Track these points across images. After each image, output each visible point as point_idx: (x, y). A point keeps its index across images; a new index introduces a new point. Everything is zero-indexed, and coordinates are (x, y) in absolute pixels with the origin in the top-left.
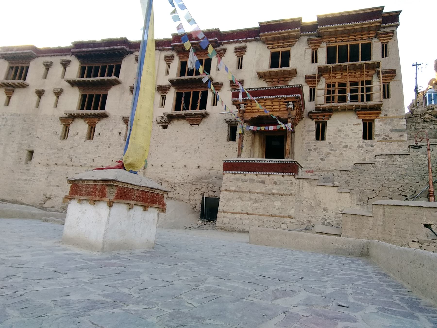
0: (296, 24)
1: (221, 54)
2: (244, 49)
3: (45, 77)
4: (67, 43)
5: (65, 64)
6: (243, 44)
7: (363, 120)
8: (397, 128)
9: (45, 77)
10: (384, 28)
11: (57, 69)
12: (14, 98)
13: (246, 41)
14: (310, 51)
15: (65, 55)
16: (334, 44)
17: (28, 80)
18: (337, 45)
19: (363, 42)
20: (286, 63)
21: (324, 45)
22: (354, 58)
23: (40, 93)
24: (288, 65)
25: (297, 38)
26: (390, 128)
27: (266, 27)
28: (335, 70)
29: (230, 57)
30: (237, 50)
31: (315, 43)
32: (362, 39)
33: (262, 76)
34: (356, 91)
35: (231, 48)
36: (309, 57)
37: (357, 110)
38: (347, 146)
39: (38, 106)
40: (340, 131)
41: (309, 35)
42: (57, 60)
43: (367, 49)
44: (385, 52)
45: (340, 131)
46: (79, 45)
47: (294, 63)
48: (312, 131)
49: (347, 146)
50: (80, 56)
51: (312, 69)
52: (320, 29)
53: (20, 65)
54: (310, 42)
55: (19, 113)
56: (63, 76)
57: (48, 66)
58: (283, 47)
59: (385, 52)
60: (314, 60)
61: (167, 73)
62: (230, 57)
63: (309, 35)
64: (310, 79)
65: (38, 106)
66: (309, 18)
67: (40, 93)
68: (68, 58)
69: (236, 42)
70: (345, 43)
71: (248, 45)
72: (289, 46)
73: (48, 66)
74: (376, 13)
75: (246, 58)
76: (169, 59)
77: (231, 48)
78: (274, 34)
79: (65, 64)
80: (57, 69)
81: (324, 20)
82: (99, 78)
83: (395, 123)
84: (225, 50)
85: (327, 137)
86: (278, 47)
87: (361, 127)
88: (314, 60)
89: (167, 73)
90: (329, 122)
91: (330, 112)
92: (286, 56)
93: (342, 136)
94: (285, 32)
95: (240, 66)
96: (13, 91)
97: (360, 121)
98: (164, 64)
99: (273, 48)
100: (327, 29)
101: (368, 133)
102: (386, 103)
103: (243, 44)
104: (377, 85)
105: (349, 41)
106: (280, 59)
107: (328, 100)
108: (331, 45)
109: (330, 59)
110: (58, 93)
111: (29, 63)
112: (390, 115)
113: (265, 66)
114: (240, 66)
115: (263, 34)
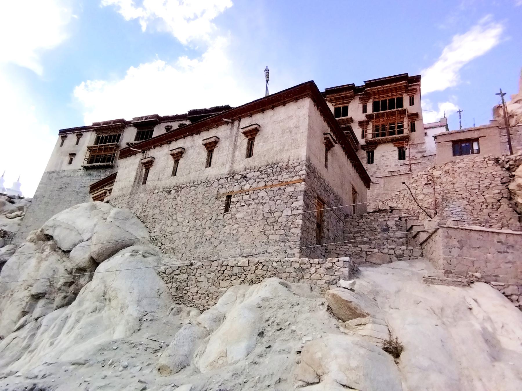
0: (351, 87)
4: (184, 111)
7: (398, 148)
8: (420, 150)
10: (411, 86)
14: (361, 106)
15: (182, 121)
16: (378, 100)
19: (397, 97)
21: (371, 100)
22: (392, 107)
24: (347, 115)
25: (352, 97)
26: (416, 151)
28: (378, 116)
31: (365, 100)
32: (396, 95)
34: (391, 128)
36: (361, 109)
37: (392, 141)
38: (388, 166)
40: (383, 156)
41: (360, 95)
44: (412, 103)
45: (383, 156)
47: (351, 114)
48: (364, 158)
49: (388, 166)
51: (362, 117)
52: (366, 91)
54: (361, 99)
58: (343, 103)
59: (412, 103)
60: (365, 110)
63: (360, 95)
64: (361, 124)
66: (359, 83)
70: (385, 99)
74: (404, 77)
78: (336, 95)
81: (369, 84)
83: (419, 147)
85: (374, 161)
86: (340, 104)
87: (397, 152)
90: (375, 151)
93: (385, 159)
94: (343, 94)
97: (396, 148)
99: (336, 105)
100: (372, 89)
101: (402, 156)
102: (413, 135)
104: (406, 122)
105: (388, 96)
107: (373, 136)
108: (376, 100)
109: (375, 109)
111: (153, 128)
112: (415, 143)
115: (328, 96)
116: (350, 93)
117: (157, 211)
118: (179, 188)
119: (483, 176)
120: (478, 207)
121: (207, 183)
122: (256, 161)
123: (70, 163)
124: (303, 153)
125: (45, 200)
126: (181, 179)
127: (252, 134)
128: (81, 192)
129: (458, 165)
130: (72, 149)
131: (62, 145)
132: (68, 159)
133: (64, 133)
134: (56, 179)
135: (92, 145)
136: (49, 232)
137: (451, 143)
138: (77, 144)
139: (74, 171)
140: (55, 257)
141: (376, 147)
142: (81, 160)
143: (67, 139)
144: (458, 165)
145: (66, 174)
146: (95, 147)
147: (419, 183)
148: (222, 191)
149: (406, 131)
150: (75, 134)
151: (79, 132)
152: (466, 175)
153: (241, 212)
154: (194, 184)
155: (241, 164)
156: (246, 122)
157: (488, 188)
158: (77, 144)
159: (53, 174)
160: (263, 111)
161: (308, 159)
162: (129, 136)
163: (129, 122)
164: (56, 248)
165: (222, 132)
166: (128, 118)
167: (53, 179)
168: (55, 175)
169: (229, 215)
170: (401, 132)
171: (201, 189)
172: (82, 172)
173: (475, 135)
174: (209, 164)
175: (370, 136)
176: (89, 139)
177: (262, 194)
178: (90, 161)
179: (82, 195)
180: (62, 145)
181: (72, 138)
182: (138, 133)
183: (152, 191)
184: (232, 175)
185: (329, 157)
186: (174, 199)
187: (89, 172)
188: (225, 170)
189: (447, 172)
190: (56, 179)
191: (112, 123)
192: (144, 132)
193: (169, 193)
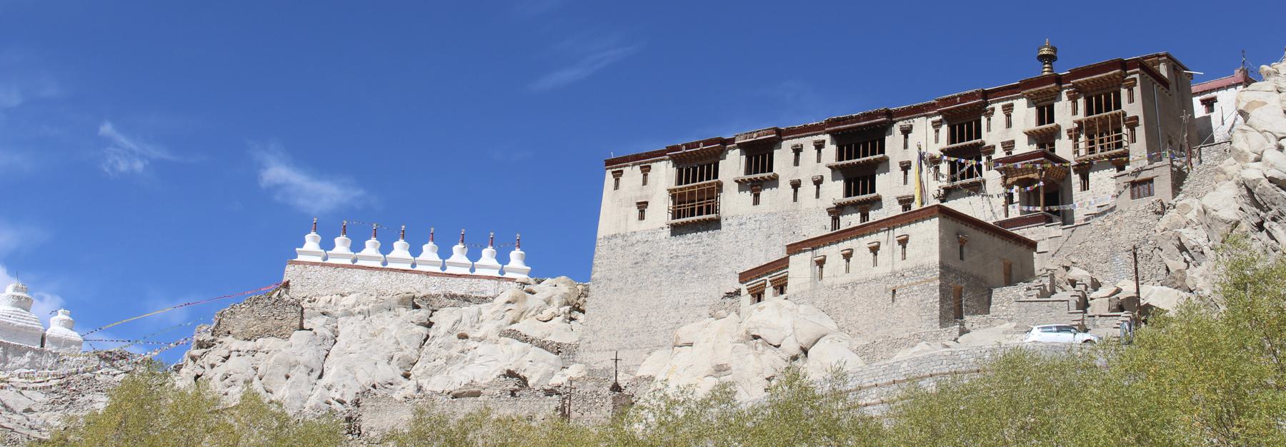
1: (989, 115)
3: (796, 163)
5: (819, 146)
9: (796, 163)
11: (809, 152)
17: (776, 169)
20: (1051, 120)
23: (796, 185)
29: (999, 116)
33: (1032, 136)
35: (998, 107)
39: (795, 199)
55: (773, 210)
56: (819, 161)
57: (797, 151)
60: (1075, 112)
61: (937, 140)
62: (999, 116)
65: (795, 199)
67: (796, 185)
68: (821, 137)
71: (1015, 102)
73: (797, 151)
76: (936, 125)
77: (998, 107)
79: (819, 146)
80: (809, 152)
82: (861, 159)
84: (993, 109)
88: (1075, 112)
89: (937, 140)
95: (1009, 124)
98: (931, 131)
110: (818, 183)
113: (1032, 125)
114: (1009, 124)
117: (839, 304)
118: (854, 284)
121: (876, 279)
122: (909, 264)
123: (642, 217)
124: (936, 259)
125: (615, 285)
126: (855, 275)
127: (903, 242)
128: (674, 267)
130: (638, 194)
134: (623, 248)
135: (673, 186)
138: (645, 183)
139: (654, 233)
140: (770, 352)
142: (661, 211)
145: (638, 237)
148: (889, 286)
149: (1125, 144)
150: (637, 168)
153: (903, 300)
154: (867, 281)
155: (900, 265)
156: (899, 232)
158: (645, 183)
159: (614, 240)
160: (910, 223)
161: (941, 263)
165: (881, 237)
167: (618, 249)
168: (619, 241)
170: (1119, 145)
171: (872, 285)
172: (667, 232)
174: (875, 263)
175: (1082, 152)
177: (915, 288)
178: (677, 214)
179: (676, 270)
183: (831, 287)
184: (894, 273)
185: (965, 250)
186: (852, 293)
188: (889, 270)
189: (1116, 223)
190: (623, 248)
193: (846, 288)
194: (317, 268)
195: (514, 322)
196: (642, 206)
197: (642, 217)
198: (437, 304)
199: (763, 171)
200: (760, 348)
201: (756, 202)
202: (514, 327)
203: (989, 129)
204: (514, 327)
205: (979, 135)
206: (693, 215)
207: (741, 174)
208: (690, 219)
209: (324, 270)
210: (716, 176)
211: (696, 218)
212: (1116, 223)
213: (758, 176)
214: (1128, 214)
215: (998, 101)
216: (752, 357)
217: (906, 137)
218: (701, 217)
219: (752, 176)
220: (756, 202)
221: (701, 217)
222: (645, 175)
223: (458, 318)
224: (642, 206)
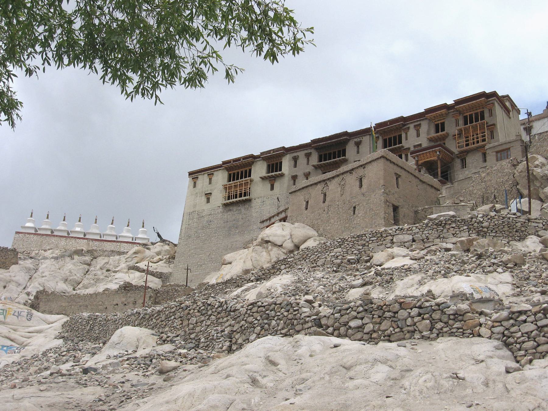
0: (445, 106)
2: (420, 125)
5: (308, 156)
6: (418, 123)
11: (302, 160)
12: (276, 185)
13: (420, 120)
18: (468, 114)
25: (447, 114)
27: (429, 111)
30: (415, 126)
35: (412, 126)
42: (301, 154)
43: (482, 114)
46: (314, 141)
50: (317, 149)
53: (275, 162)
56: (308, 164)
57: (295, 159)
60: (457, 124)
62: (412, 132)
66: (450, 102)
69: (414, 122)
71: (421, 122)
72: (444, 119)
73: (295, 159)
75: (421, 131)
77: (412, 126)
79: (308, 156)
80: (302, 160)
81: (458, 102)
84: (409, 128)
86: (438, 121)
90: (467, 159)
91: (467, 152)
92: (443, 124)
95: (418, 135)
96: (275, 180)
103: (418, 123)
106: (440, 127)
116: (444, 111)
119: (505, 174)
120: (501, 193)
123: (208, 200)
129: (494, 169)
131: (195, 186)
132: (204, 199)
133: (194, 175)
136: (267, 239)
137: (495, 153)
140: (275, 249)
141: (467, 154)
142: (219, 198)
143: (199, 179)
144: (494, 169)
146: (229, 184)
147: (474, 183)
150: (206, 175)
151: (210, 171)
152: (497, 175)
157: (507, 181)
162: (259, 170)
163: (258, 157)
164: (275, 245)
166: (257, 153)
169: (355, 216)
172: (221, 210)
173: (504, 147)
176: (221, 178)
180: (195, 186)
181: (203, 180)
182: (269, 166)
186: (328, 213)
187: (228, 208)
189: (488, 174)
191: (242, 160)
192: (273, 165)
194: (32, 236)
195: (137, 263)
196: (208, 196)
197: (208, 200)
198: (96, 254)
199: (276, 171)
200: (270, 247)
201: (272, 188)
202: (137, 265)
203: (407, 139)
204: (137, 265)
205: (400, 142)
206: (236, 198)
207: (264, 173)
208: (235, 200)
209: (35, 237)
210: (250, 176)
211: (238, 199)
212: (488, 174)
213: (273, 174)
214: (496, 168)
215: (412, 123)
216: (264, 253)
217: (358, 147)
218: (241, 199)
219: (269, 175)
220: (272, 188)
221: (241, 199)
222: (210, 179)
223: (107, 261)
224: (208, 196)
